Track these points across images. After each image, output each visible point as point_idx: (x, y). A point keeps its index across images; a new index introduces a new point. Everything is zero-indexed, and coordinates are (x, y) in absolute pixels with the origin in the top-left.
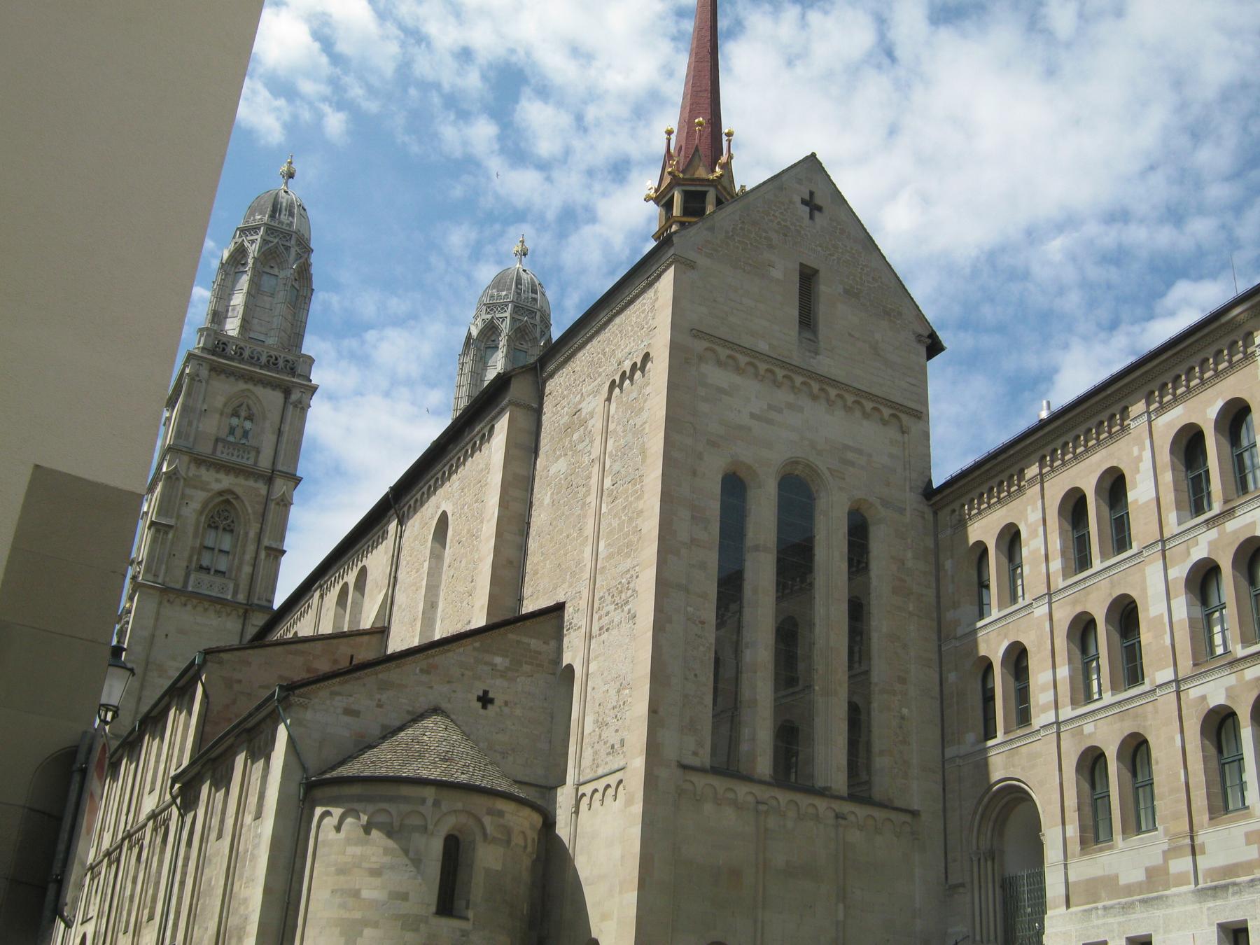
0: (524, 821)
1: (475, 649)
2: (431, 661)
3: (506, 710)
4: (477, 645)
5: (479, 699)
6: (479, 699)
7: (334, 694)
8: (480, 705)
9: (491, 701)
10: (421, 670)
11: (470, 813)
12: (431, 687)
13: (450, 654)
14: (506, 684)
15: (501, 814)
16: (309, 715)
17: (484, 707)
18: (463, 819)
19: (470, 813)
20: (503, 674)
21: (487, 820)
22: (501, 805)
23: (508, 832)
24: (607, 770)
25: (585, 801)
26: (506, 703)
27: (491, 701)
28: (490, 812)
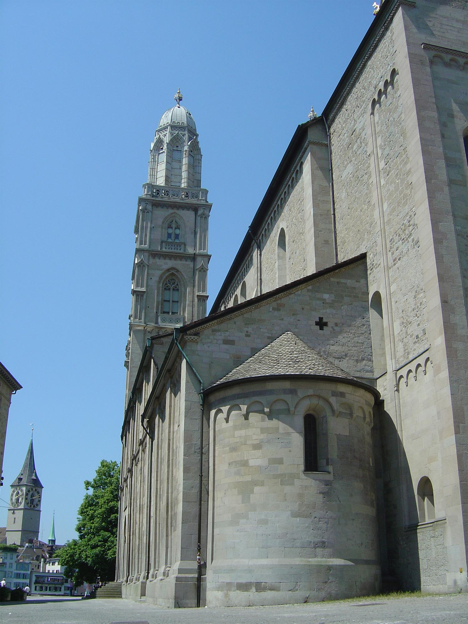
0: (360, 399)
1: (308, 290)
2: (279, 302)
3: (337, 329)
4: (310, 288)
5: (317, 324)
6: (317, 324)
7: (214, 331)
8: (318, 327)
9: (326, 324)
10: (273, 309)
11: (319, 397)
12: (282, 319)
13: (292, 296)
14: (334, 312)
15: (342, 395)
16: (199, 347)
17: (321, 329)
18: (315, 401)
19: (319, 397)
20: (331, 305)
21: (333, 400)
22: (342, 388)
23: (350, 407)
24: (415, 356)
25: (403, 381)
26: (336, 325)
27: (326, 324)
28: (334, 394)
